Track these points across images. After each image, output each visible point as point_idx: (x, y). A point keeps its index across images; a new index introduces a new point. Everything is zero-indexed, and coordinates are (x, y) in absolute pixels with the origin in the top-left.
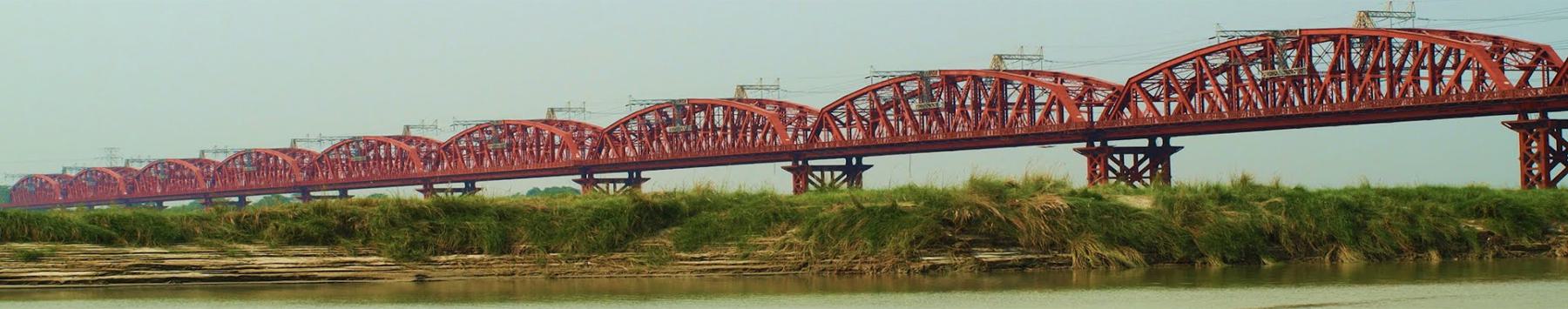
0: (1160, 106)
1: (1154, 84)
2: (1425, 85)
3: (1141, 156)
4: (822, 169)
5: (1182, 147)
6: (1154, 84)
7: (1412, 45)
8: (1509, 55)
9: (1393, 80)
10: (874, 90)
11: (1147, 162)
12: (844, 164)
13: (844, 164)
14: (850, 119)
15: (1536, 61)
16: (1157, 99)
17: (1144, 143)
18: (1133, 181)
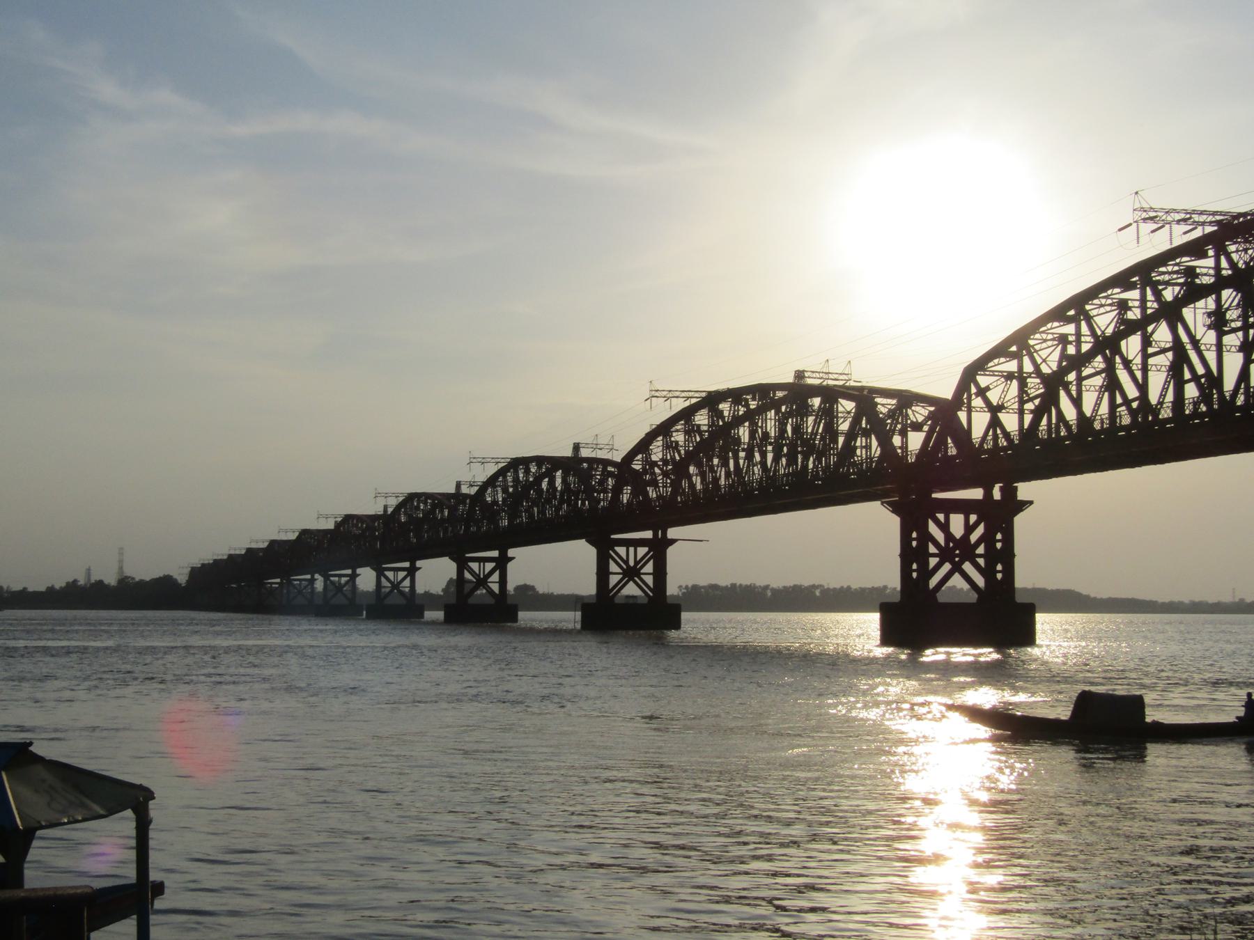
4: (627, 543)
5: (1031, 503)
11: (980, 530)
17: (976, 494)
18: (962, 562)
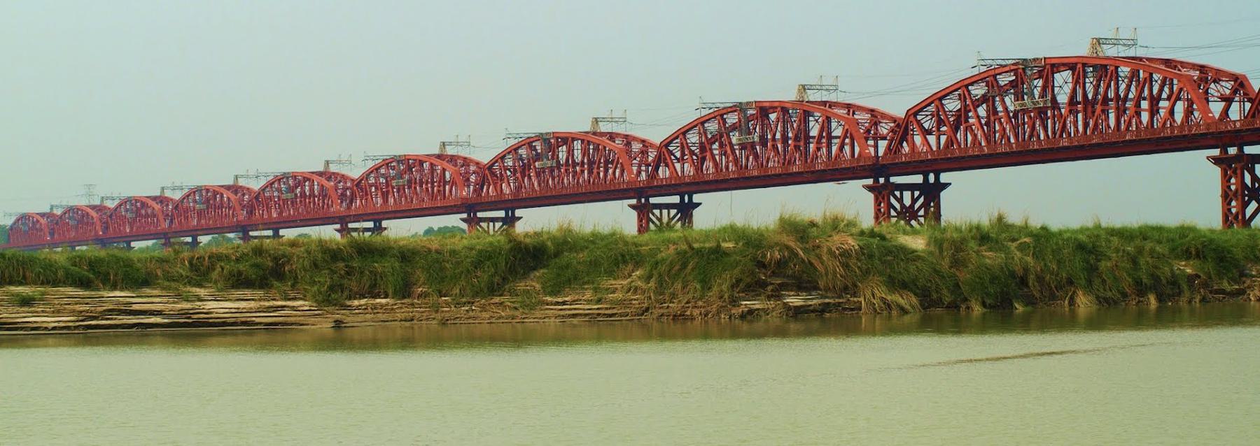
0: (932, 139)
1: (927, 116)
2: (1145, 117)
3: (917, 193)
5: (950, 184)
6: (927, 116)
7: (1134, 74)
8: (1212, 85)
9: (1120, 112)
10: (702, 122)
11: (922, 200)
12: (678, 202)
13: (678, 202)
14: (683, 154)
15: (1235, 91)
16: (929, 132)
17: (918, 179)
18: (910, 220)
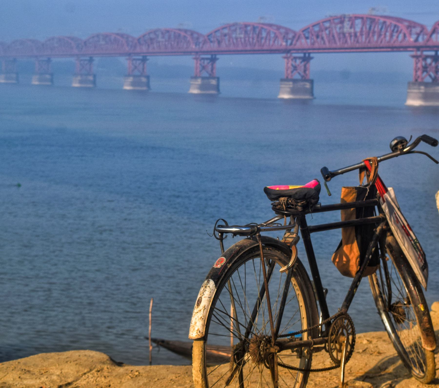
0: (309, 41)
2: (388, 38)
16: (307, 38)
